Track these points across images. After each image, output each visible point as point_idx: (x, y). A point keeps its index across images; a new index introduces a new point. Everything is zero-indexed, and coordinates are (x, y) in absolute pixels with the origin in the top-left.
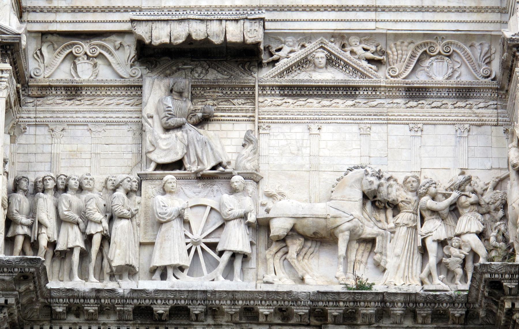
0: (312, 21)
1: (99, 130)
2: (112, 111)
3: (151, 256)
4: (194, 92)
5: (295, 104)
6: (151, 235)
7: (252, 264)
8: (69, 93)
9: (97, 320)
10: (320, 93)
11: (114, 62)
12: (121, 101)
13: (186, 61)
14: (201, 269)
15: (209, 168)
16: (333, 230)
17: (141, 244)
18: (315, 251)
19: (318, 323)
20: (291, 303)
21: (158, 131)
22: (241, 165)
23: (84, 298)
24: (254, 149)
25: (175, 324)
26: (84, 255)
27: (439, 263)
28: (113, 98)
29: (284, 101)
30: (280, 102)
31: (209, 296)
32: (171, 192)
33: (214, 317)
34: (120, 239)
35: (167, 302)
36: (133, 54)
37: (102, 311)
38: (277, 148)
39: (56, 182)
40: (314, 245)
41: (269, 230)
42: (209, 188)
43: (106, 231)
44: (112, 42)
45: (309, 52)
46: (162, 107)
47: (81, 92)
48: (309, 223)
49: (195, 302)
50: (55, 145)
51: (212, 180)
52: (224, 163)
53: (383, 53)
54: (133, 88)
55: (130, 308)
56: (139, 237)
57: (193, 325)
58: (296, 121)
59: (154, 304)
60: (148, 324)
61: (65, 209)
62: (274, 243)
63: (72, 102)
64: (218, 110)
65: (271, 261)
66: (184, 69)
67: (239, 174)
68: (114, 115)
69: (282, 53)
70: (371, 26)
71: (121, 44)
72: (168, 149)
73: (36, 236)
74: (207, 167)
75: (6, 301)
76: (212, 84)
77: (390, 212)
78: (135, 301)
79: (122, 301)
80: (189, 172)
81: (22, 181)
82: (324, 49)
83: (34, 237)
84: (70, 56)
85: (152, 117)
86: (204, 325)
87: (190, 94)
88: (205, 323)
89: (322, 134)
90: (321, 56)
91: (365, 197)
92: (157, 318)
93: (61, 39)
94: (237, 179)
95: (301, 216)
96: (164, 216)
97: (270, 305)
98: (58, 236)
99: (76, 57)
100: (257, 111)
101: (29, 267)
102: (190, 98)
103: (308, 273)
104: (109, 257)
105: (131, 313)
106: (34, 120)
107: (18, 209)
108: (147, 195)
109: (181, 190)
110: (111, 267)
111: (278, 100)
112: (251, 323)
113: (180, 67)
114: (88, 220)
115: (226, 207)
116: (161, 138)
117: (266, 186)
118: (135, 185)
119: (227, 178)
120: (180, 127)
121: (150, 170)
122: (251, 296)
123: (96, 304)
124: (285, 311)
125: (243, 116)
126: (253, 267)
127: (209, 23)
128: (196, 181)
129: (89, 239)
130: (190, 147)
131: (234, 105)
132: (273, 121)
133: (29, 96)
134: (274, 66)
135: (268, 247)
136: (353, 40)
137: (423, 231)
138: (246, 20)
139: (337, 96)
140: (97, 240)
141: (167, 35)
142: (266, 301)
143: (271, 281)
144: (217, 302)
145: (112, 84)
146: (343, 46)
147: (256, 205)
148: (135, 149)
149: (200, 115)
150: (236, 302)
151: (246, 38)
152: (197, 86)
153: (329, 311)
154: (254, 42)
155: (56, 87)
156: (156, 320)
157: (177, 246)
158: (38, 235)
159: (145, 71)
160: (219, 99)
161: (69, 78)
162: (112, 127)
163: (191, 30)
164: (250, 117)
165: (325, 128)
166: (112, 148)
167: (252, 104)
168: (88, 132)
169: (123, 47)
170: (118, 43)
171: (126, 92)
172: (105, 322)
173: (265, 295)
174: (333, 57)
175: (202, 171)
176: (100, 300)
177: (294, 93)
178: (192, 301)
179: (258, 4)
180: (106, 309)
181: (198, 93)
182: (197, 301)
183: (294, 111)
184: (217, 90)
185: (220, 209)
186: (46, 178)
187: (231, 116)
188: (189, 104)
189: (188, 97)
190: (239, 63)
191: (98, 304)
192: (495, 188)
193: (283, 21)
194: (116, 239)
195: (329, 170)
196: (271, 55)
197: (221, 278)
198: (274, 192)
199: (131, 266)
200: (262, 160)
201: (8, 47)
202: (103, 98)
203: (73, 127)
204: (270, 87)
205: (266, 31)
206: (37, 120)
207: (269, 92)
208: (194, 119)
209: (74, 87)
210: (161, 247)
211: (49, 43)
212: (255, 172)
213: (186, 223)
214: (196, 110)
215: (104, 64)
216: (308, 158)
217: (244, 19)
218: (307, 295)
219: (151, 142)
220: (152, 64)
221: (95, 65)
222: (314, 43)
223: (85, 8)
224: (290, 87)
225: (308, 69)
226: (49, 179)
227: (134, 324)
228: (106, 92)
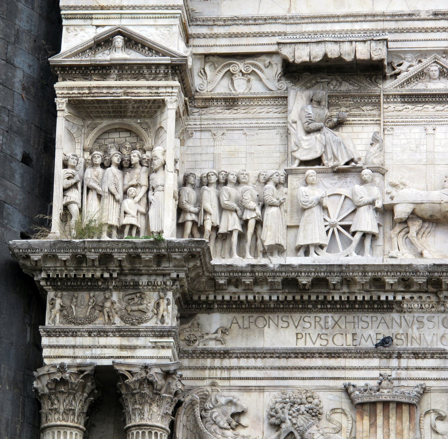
0: (427, 40)
1: (253, 134)
2: (263, 118)
3: (296, 236)
4: (330, 101)
5: (414, 110)
6: (296, 219)
7: (380, 242)
8: (228, 104)
9: (252, 290)
10: (434, 100)
11: (265, 77)
12: (271, 110)
13: (323, 76)
14: (338, 246)
15: (343, 163)
16: (446, 213)
17: (288, 227)
18: (432, 231)
19: (434, 290)
20: (411, 274)
21: (301, 133)
22: (370, 161)
23: (242, 272)
24: (380, 147)
25: (316, 293)
26: (242, 236)
28: (264, 107)
29: (405, 107)
30: (401, 108)
31: (344, 269)
32: (312, 184)
33: (349, 286)
34: (271, 223)
35: (309, 274)
36: (280, 71)
37: (256, 282)
38: (399, 146)
39: (218, 177)
40: (431, 226)
42: (344, 180)
43: (259, 216)
44: (262, 61)
45: (425, 66)
46: (304, 114)
47: (238, 103)
48: (426, 207)
49: (332, 274)
50: (217, 146)
51: (346, 174)
52: (356, 159)
54: (280, 99)
55: (279, 280)
56: (286, 221)
57: (332, 293)
58: (415, 124)
59: (299, 276)
60: (294, 293)
61: (225, 199)
62: (397, 225)
63: (230, 111)
64: (351, 115)
65: (395, 239)
66: (322, 82)
67: (368, 168)
68: (265, 121)
69: (402, 68)
71: (270, 63)
72: (309, 148)
73: (202, 221)
74: (341, 164)
75: (178, 276)
76: (345, 94)
78: (284, 274)
79: (273, 274)
80: (327, 167)
81: (190, 177)
82: (438, 63)
83: (201, 222)
84: (228, 73)
85: (295, 122)
86: (340, 293)
87: (327, 103)
88: (341, 291)
89: (436, 134)
90: (435, 69)
92: (301, 287)
93: (221, 59)
94: (366, 173)
95: (419, 202)
96: (306, 204)
97: (395, 276)
98: (220, 221)
99: (233, 74)
100: (382, 115)
101: (196, 248)
102: (327, 106)
103: (426, 249)
104: (262, 238)
105: (281, 284)
106: (199, 126)
107: (187, 200)
108: (293, 187)
109: (320, 182)
110: (263, 246)
111: (399, 107)
112: (379, 291)
113: (319, 80)
114: (244, 208)
115: (358, 196)
116: (303, 140)
117: (391, 177)
118: (282, 179)
119: (358, 172)
120: (318, 130)
121: (295, 166)
122: (379, 269)
123: (251, 276)
124: (407, 280)
125: (371, 120)
126: (380, 244)
127: (341, 44)
128: (333, 174)
129: (245, 224)
130: (327, 146)
131: (364, 111)
132: (395, 124)
133: (195, 107)
134: (396, 78)
135: (393, 227)
138: (372, 41)
140: (252, 224)
141: (308, 55)
142: (391, 273)
143: (395, 256)
144: (351, 274)
145: (263, 96)
147: (382, 194)
149: (335, 120)
150: (367, 274)
151: (373, 55)
152: (333, 96)
153: (443, 280)
154: (379, 59)
155: (217, 99)
156: (300, 290)
157: (317, 228)
158: (204, 220)
159: (290, 85)
160: (351, 106)
161: (228, 91)
162: (263, 131)
163: (327, 50)
164: (377, 120)
165: (438, 129)
166: (263, 148)
167: (378, 110)
168: (244, 136)
169: (272, 65)
170: (267, 62)
171: (275, 102)
172: (259, 291)
173: (390, 268)
174: (445, 70)
175: (337, 166)
176: (255, 273)
177: (413, 100)
178: (330, 273)
179: (382, 27)
180: (260, 281)
181: (333, 101)
182: (334, 273)
183: (413, 115)
184: (349, 99)
185: (353, 198)
186: (210, 174)
187: (361, 120)
188: (327, 111)
189: (325, 106)
190: (367, 76)
191: (253, 277)
193: (403, 41)
194: (267, 223)
195: (443, 163)
196: (394, 69)
197: (354, 254)
198: (397, 183)
199: (280, 245)
200: (387, 156)
201: (177, 68)
202: (255, 107)
203: (231, 132)
204: (393, 96)
205: (389, 50)
206: (202, 126)
207: (392, 100)
208: (330, 124)
209: (232, 99)
210: (304, 229)
211: (211, 63)
212: (381, 166)
213: (325, 209)
214: (332, 116)
215: (256, 80)
216: (425, 154)
217: (370, 40)
218: (425, 267)
219: (295, 143)
220: (295, 78)
221: (249, 81)
222: (429, 58)
223: (240, 34)
224: (410, 96)
225: (424, 80)
226: (212, 175)
227: (283, 293)
228: (258, 103)
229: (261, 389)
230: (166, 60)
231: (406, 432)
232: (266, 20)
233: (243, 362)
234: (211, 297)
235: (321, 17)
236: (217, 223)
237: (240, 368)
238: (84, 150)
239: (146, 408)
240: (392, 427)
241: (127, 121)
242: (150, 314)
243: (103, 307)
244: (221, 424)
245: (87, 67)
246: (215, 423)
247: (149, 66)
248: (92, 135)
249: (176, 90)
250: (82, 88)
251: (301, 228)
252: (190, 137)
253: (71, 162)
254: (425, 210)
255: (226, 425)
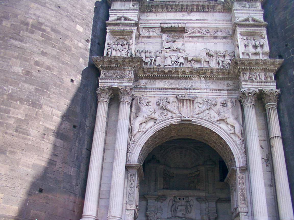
3: (164, 64)
17: (162, 62)
21: (165, 42)
27: (222, 65)
36: (160, 31)
41: (187, 59)
53: (209, 31)
55: (160, 71)
58: (192, 42)
70: (206, 26)
74: (175, 49)
77: (211, 57)
90: (197, 31)
91: (207, 54)
94: (181, 51)
111: (189, 39)
120: (170, 42)
129: (152, 60)
136: (203, 29)
137: (218, 59)
139: (200, 38)
146: (201, 30)
148: (161, 46)
192: (232, 53)
213: (171, 58)
221: (153, 33)
224: (191, 36)
229: (154, 96)
230: (134, 22)
231: (192, 107)
232: (157, 20)
233: (150, 90)
234: (143, 75)
235: (170, 20)
236: (145, 60)
237: (149, 92)
238: (113, 42)
239: (125, 97)
240: (188, 105)
241: (123, 36)
242: (127, 76)
243: (115, 74)
244: (144, 104)
245: (115, 24)
246: (143, 104)
247: (130, 23)
248: (116, 39)
249: (136, 29)
250: (113, 28)
251: (165, 62)
252: (139, 44)
253: (109, 44)
254: (195, 58)
255: (145, 104)
